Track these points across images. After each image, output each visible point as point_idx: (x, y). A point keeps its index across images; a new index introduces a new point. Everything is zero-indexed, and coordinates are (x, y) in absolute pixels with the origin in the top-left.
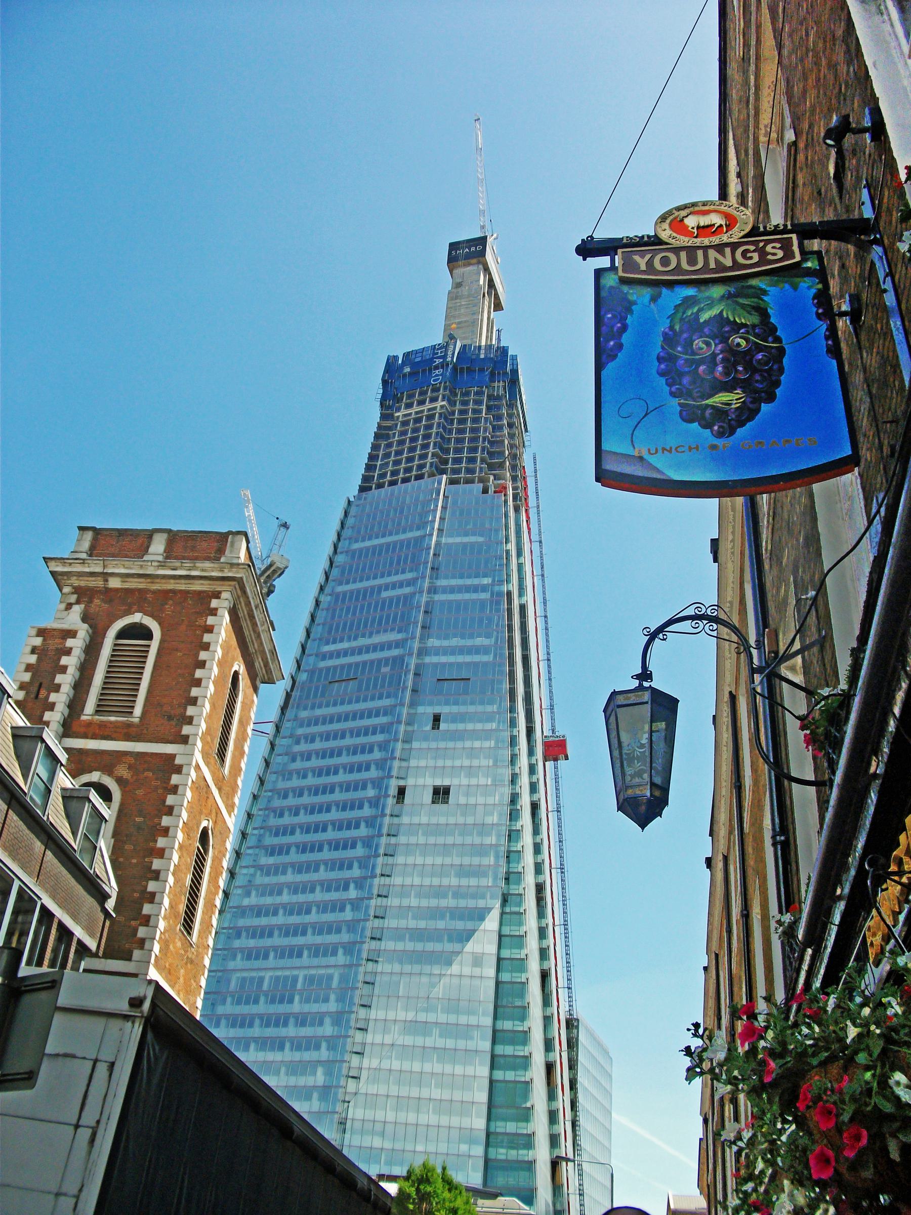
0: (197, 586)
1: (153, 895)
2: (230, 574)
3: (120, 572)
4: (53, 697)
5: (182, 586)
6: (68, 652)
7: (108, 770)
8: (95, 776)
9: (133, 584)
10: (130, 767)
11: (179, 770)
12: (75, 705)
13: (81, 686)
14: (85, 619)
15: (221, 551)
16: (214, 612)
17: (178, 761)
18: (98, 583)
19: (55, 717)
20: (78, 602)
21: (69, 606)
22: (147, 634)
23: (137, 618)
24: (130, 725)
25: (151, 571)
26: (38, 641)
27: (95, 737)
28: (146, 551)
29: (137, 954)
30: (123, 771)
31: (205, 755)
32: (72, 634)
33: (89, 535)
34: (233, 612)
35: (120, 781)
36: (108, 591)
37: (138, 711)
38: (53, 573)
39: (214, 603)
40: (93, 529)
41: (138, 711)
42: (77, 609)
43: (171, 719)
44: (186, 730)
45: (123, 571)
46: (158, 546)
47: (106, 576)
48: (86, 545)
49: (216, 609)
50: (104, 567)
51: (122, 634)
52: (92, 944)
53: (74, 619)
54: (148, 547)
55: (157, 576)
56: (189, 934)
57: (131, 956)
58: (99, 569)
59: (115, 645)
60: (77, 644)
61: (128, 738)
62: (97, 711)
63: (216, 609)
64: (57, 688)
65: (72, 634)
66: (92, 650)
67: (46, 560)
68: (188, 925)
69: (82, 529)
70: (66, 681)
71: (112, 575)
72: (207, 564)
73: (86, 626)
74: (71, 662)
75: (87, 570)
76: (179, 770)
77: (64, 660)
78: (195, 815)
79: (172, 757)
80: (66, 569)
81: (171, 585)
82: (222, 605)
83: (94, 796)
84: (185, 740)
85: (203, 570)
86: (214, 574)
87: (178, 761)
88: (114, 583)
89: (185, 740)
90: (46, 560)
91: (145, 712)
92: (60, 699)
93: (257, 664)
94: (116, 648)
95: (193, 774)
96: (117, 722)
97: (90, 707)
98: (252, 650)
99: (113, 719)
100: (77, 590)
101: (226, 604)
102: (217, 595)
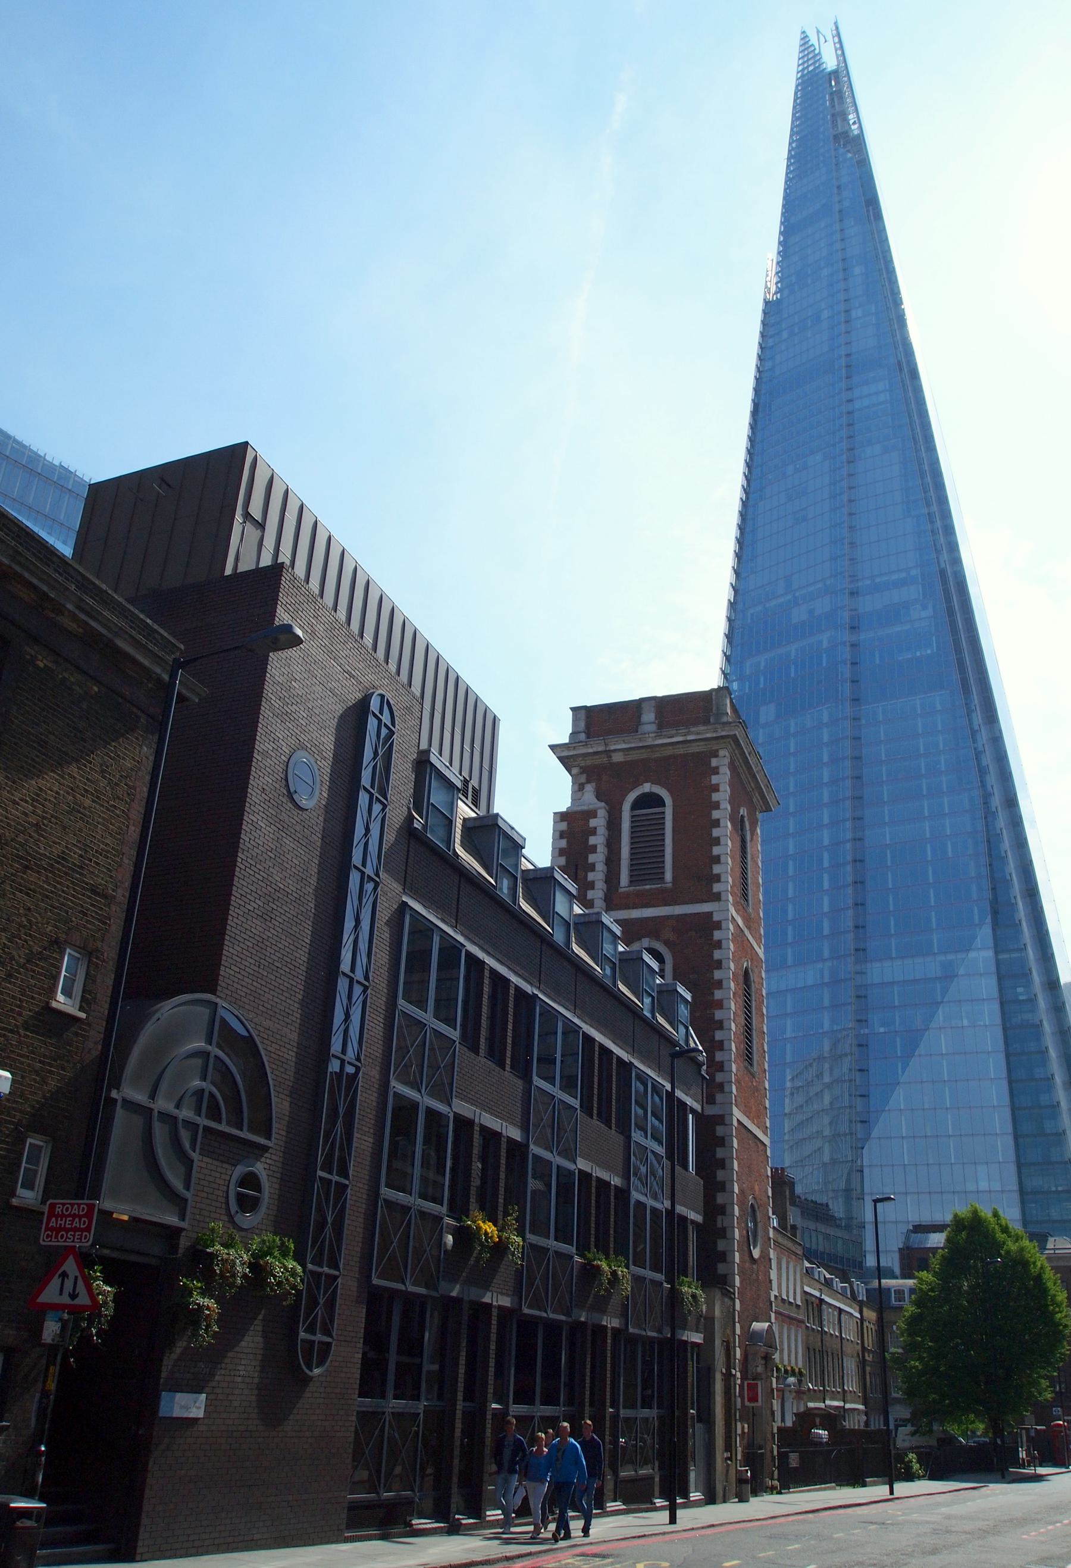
0: (695, 749)
1: (721, 1042)
2: (724, 733)
3: (620, 747)
4: (591, 876)
5: (680, 751)
6: (594, 832)
7: (655, 935)
8: (646, 942)
9: (635, 756)
11: (718, 926)
12: (612, 877)
14: (599, 797)
16: (716, 771)
17: (716, 918)
20: (588, 781)
22: (659, 802)
23: (647, 788)
24: (663, 891)
25: (649, 742)
26: (564, 826)
28: (639, 723)
29: (719, 1097)
32: (593, 814)
33: (583, 712)
34: (732, 766)
35: (667, 943)
37: (668, 876)
38: (558, 758)
39: (714, 762)
40: (585, 707)
41: (668, 876)
42: (590, 788)
43: (699, 879)
44: (717, 888)
45: (624, 746)
46: (649, 716)
47: (608, 753)
48: (582, 725)
49: (717, 768)
50: (606, 745)
51: (635, 806)
52: (697, 1107)
54: (640, 717)
55: (657, 745)
56: (751, 1065)
57: (714, 1099)
59: (632, 817)
60: (599, 822)
62: (631, 882)
63: (717, 768)
64: (592, 868)
65: (593, 814)
66: (613, 825)
67: (553, 747)
69: (573, 709)
70: (598, 858)
71: (615, 750)
72: (701, 728)
73: (603, 804)
74: (598, 840)
75: (590, 750)
76: (718, 926)
77: (592, 840)
79: (710, 914)
80: (571, 753)
81: (669, 752)
82: (722, 762)
83: (647, 958)
84: (717, 897)
85: (698, 734)
86: (709, 735)
87: (716, 918)
88: (617, 758)
89: (717, 897)
90: (553, 747)
92: (597, 876)
93: (755, 800)
94: (634, 819)
95: (731, 927)
96: (651, 889)
98: (749, 789)
99: (648, 887)
100: (584, 770)
101: (727, 761)
102: (715, 754)
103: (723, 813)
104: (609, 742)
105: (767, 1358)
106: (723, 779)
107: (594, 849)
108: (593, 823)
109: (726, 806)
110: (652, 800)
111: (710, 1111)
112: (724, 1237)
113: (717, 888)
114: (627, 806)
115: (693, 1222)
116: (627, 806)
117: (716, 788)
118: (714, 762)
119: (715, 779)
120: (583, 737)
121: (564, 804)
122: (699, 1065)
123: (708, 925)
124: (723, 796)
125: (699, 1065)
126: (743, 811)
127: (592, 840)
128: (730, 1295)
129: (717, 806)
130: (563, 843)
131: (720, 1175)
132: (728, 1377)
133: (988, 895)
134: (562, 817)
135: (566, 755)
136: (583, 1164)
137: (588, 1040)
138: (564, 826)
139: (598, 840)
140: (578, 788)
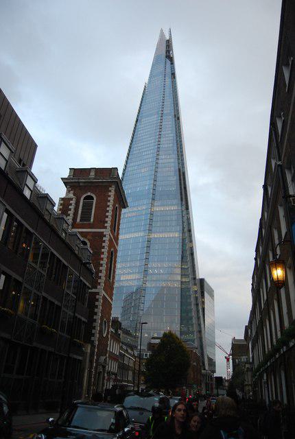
0: (104, 184)
5: (101, 184)
6: (71, 204)
11: (105, 236)
12: (74, 219)
13: (75, 214)
15: (110, 174)
18: (77, 184)
19: (70, 222)
21: (69, 191)
23: (89, 194)
26: (62, 202)
27: (81, 228)
29: (98, 287)
30: (89, 237)
31: (111, 231)
32: (72, 199)
34: (115, 191)
36: (80, 186)
37: (92, 220)
39: (110, 189)
41: (92, 220)
42: (72, 192)
43: (101, 222)
44: (106, 225)
51: (84, 199)
53: (71, 195)
60: (73, 202)
65: (72, 199)
67: (62, 179)
68: (110, 278)
70: (71, 213)
76: (105, 236)
82: (113, 189)
84: (106, 228)
89: (106, 228)
90: (62, 179)
91: (94, 221)
97: (78, 220)
100: (71, 187)
103: (111, 204)
104: (79, 180)
105: (104, 367)
106: (112, 194)
107: (70, 210)
110: (90, 198)
111: (94, 290)
114: (82, 199)
116: (82, 199)
118: (110, 189)
121: (63, 195)
122: (93, 274)
123: (102, 235)
124: (111, 199)
125: (93, 274)
128: (93, 346)
129: (109, 201)
130: (61, 207)
131: (96, 310)
132: (90, 372)
133: (181, 253)
134: (62, 199)
135: (66, 182)
136: (44, 294)
137: (52, 253)
138: (62, 202)
140: (68, 192)
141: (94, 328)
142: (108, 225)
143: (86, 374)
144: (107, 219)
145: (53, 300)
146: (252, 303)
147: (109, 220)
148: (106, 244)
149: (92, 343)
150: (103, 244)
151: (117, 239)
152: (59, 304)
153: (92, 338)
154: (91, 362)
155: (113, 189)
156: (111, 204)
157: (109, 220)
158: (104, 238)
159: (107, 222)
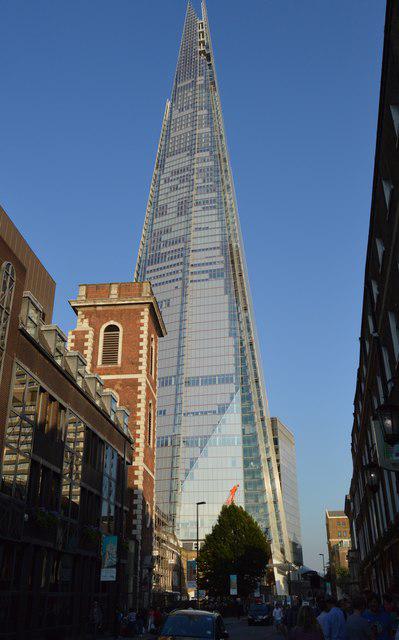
6: (87, 340)
10: (121, 385)
11: (140, 384)
13: (95, 353)
16: (142, 317)
23: (112, 323)
24: (117, 368)
28: (109, 294)
30: (117, 387)
32: (87, 332)
35: (117, 391)
39: (142, 314)
41: (119, 362)
42: (86, 321)
43: (132, 364)
44: (140, 368)
46: (114, 291)
47: (95, 306)
58: (92, 304)
60: (90, 336)
61: (118, 373)
65: (87, 332)
66: (96, 338)
70: (88, 352)
74: (89, 344)
76: (140, 384)
77: (86, 344)
78: (147, 399)
84: (140, 372)
89: (140, 372)
106: (145, 320)
108: (86, 336)
109: (146, 332)
112: (135, 518)
113: (140, 368)
115: (126, 512)
117: (142, 325)
118: (142, 314)
119: (142, 321)
120: (84, 298)
123: (135, 383)
126: (153, 336)
127: (86, 344)
139: (89, 344)
141: (135, 517)
142: (143, 368)
143: (132, 583)
144: (141, 360)
145: (92, 490)
146: (352, 474)
147: (143, 360)
148: (142, 397)
149: (134, 538)
150: (139, 397)
151: (154, 384)
152: (99, 493)
153: (134, 532)
154: (136, 565)
155: (146, 313)
156: (144, 336)
157: (143, 360)
158: (139, 388)
159: (141, 364)
